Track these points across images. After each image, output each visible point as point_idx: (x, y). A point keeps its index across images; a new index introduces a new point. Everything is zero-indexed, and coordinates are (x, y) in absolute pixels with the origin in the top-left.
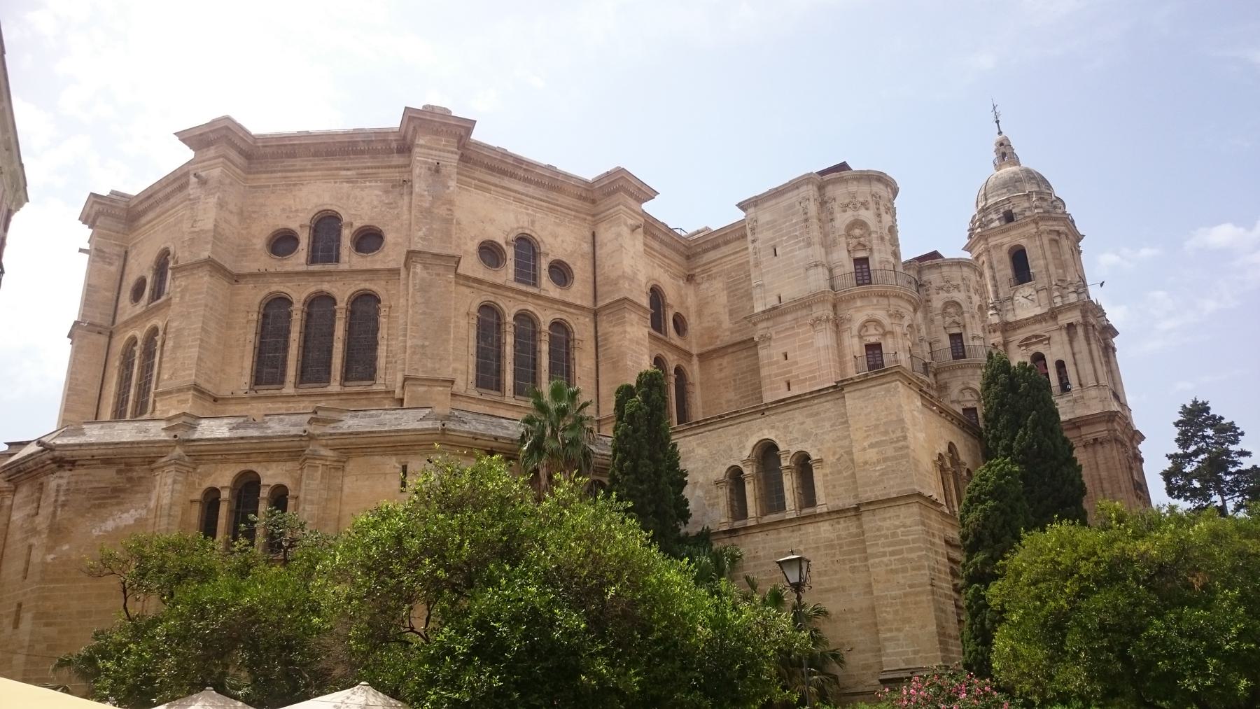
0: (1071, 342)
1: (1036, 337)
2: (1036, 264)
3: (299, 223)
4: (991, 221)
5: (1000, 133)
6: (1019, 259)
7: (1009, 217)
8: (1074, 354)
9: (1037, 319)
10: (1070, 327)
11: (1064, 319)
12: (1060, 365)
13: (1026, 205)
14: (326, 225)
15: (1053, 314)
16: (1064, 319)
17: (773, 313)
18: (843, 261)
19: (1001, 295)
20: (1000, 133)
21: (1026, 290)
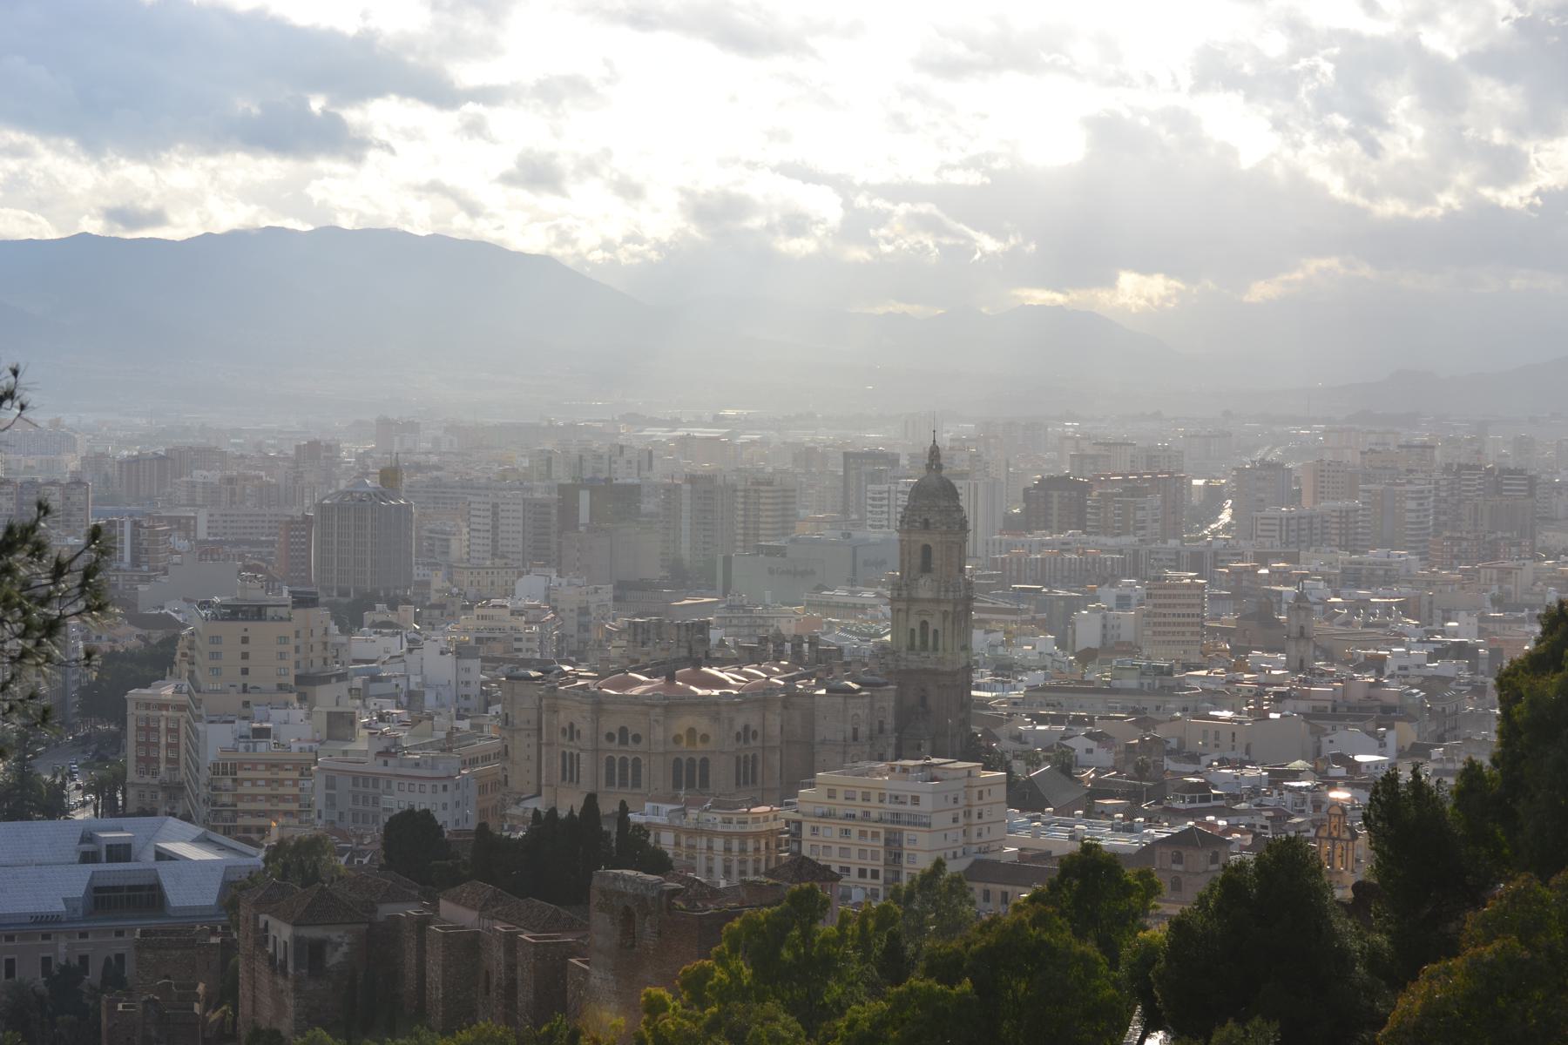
0: (944, 621)
1: (926, 611)
2: (936, 562)
3: (682, 732)
4: (915, 521)
5: (934, 441)
6: (927, 550)
7: (926, 524)
8: (944, 629)
9: (929, 600)
10: (945, 614)
11: (944, 607)
12: (936, 632)
13: (938, 518)
14: (691, 732)
15: (937, 601)
16: (944, 607)
17: (824, 742)
18: (850, 733)
19: (912, 575)
20: (934, 441)
21: (925, 581)
